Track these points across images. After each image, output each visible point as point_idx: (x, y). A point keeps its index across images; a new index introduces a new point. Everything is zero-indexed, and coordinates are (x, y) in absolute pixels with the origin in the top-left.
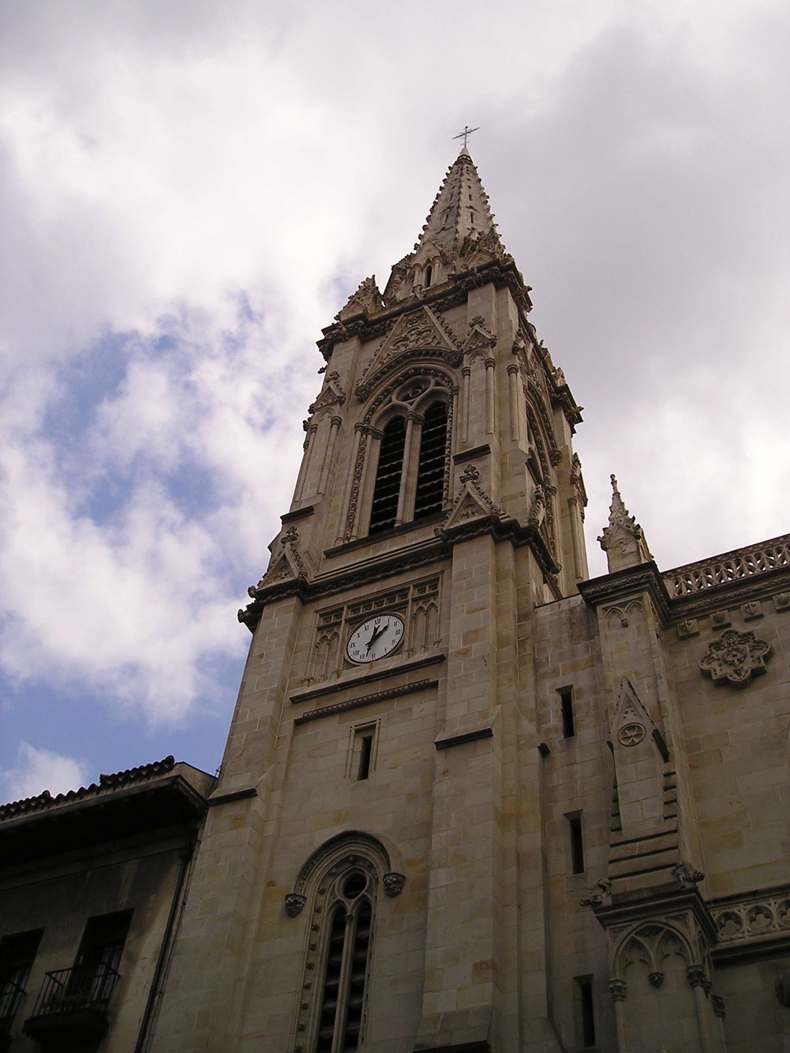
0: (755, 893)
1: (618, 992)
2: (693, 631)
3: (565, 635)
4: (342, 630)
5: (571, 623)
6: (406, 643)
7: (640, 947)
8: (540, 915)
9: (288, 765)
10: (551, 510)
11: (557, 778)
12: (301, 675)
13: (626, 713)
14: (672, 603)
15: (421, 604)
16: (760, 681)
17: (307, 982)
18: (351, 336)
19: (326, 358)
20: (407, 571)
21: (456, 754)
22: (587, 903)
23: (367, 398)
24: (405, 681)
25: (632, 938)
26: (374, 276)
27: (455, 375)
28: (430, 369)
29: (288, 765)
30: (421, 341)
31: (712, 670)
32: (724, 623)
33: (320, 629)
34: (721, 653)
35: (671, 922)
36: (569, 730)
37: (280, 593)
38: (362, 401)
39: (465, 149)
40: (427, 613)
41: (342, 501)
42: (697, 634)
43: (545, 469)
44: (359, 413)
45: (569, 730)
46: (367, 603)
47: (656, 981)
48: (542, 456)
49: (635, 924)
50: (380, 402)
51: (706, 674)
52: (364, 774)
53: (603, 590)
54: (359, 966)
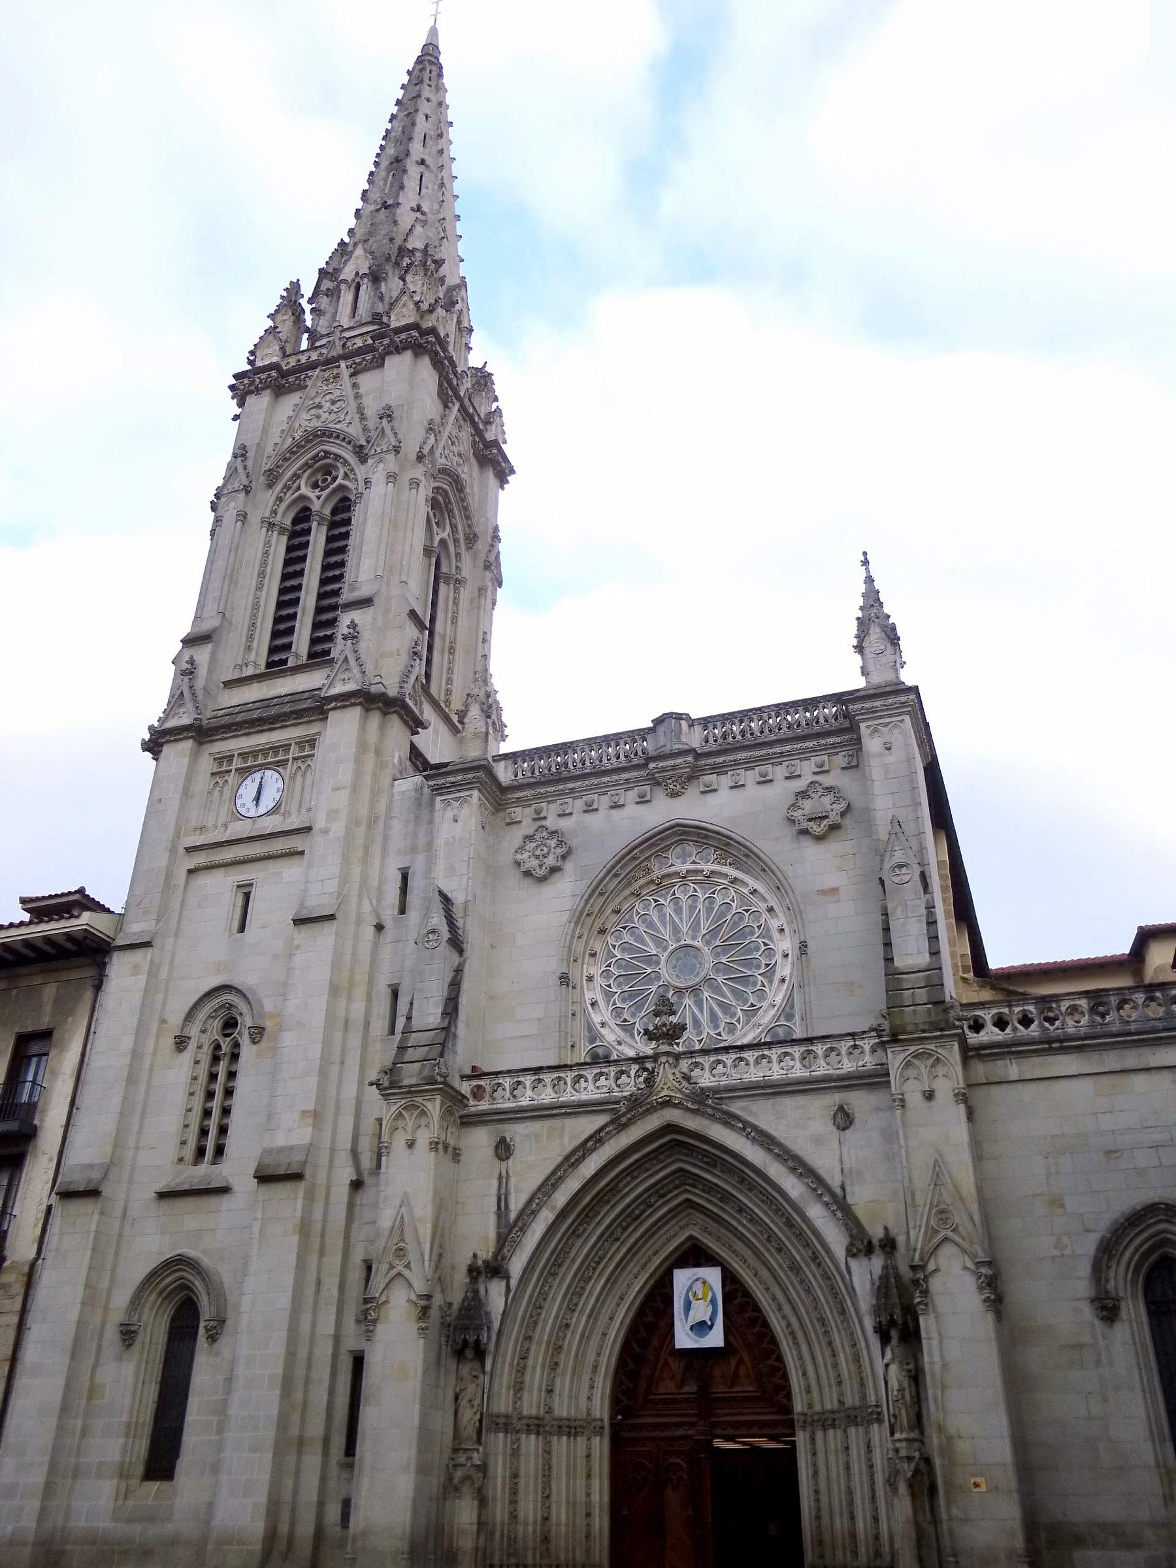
3: (412, 816)
4: (231, 778)
5: (418, 803)
6: (283, 804)
9: (181, 912)
10: (457, 607)
11: (386, 953)
12: (194, 822)
14: (504, 790)
15: (300, 764)
16: (557, 876)
17: (189, 1107)
18: (263, 389)
19: (241, 404)
20: (291, 725)
21: (306, 931)
23: (274, 483)
24: (279, 845)
26: (298, 280)
27: (361, 472)
28: (341, 457)
29: (181, 912)
30: (333, 416)
32: (542, 815)
33: (213, 774)
34: (534, 845)
36: (402, 911)
37: (178, 734)
38: (270, 486)
39: (434, 32)
40: (304, 776)
41: (241, 618)
42: (520, 822)
43: (458, 555)
44: (265, 501)
45: (402, 911)
46: (254, 754)
47: (411, 1144)
48: (456, 541)
49: (404, 1101)
50: (289, 489)
51: (518, 864)
52: (242, 929)
54: (229, 1093)
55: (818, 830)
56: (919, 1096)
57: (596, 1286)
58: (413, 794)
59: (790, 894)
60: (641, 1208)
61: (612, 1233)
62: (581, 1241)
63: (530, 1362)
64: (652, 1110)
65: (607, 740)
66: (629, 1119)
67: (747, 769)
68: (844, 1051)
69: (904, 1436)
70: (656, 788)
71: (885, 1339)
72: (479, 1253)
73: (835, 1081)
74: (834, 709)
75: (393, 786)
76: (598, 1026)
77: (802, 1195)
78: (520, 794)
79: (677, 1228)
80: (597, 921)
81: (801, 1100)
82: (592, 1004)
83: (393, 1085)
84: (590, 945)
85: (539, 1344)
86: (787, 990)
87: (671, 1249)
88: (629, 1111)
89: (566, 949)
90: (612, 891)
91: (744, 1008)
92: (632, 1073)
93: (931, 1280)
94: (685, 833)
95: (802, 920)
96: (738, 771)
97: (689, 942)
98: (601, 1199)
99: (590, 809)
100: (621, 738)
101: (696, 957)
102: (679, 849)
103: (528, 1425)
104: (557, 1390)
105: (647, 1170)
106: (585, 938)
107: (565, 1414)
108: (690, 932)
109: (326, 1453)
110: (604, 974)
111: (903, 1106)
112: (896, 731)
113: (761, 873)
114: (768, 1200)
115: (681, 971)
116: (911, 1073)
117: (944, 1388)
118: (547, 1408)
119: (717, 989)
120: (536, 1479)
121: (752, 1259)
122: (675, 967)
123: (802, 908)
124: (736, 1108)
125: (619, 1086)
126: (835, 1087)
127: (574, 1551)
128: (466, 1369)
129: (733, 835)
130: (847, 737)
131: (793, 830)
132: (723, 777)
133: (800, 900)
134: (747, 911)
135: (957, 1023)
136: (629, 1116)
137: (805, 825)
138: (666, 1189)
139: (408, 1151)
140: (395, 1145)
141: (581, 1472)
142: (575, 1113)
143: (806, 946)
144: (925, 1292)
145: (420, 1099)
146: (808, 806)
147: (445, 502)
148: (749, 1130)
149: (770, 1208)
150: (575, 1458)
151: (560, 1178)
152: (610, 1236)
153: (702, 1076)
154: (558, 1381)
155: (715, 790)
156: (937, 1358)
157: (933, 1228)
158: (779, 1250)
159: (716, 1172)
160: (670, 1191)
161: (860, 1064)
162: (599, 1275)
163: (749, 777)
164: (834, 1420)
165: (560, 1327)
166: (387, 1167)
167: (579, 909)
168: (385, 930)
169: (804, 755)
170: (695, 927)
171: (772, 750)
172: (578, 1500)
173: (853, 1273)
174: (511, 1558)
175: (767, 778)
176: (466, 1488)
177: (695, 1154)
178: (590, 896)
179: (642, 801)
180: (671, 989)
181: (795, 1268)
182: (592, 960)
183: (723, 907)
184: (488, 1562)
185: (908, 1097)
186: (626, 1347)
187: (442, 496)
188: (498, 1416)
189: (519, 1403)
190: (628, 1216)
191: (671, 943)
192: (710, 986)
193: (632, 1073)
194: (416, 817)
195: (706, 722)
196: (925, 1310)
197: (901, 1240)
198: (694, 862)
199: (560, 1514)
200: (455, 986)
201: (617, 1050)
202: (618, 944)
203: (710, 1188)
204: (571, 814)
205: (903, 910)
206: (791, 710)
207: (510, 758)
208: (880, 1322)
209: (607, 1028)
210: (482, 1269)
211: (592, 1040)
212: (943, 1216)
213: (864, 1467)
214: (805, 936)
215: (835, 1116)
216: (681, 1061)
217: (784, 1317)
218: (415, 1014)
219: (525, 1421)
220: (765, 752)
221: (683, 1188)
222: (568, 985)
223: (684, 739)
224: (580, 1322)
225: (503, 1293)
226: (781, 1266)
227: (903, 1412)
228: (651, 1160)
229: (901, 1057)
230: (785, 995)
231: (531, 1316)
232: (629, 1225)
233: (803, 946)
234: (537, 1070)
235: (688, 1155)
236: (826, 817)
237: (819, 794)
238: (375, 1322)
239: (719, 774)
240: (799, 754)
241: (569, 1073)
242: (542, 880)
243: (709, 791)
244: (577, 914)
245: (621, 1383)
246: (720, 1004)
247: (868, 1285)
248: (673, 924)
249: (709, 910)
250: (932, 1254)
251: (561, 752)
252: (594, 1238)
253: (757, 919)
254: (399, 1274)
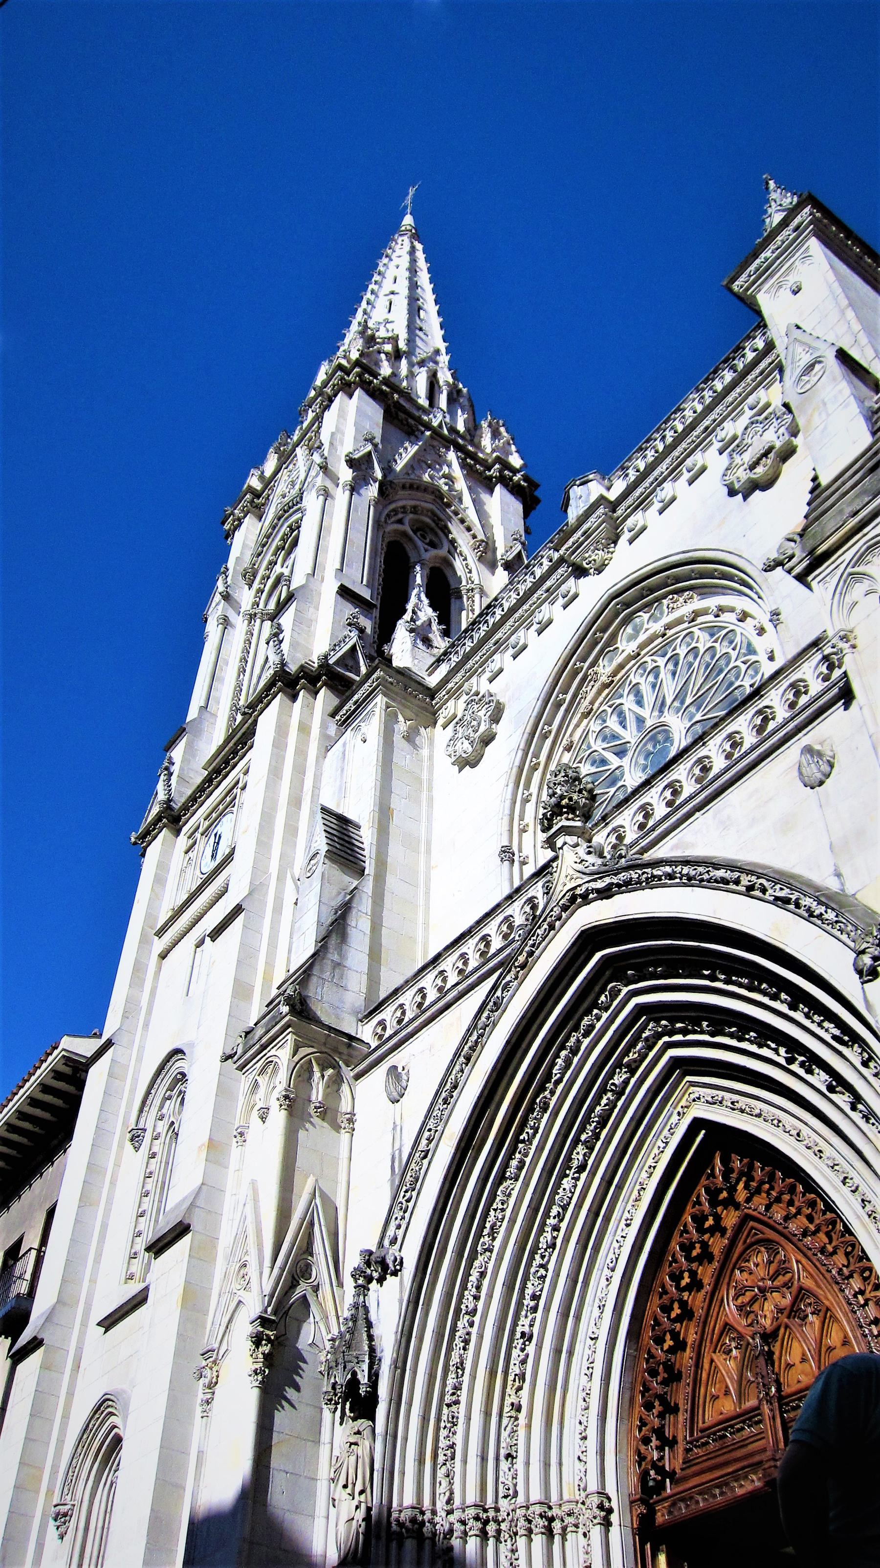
61: (569, 1158)
134: (715, 641)
147: (434, 521)
163: (677, 487)
187: (427, 516)
190: (587, 1120)
207: (443, 660)
221: (660, 1043)
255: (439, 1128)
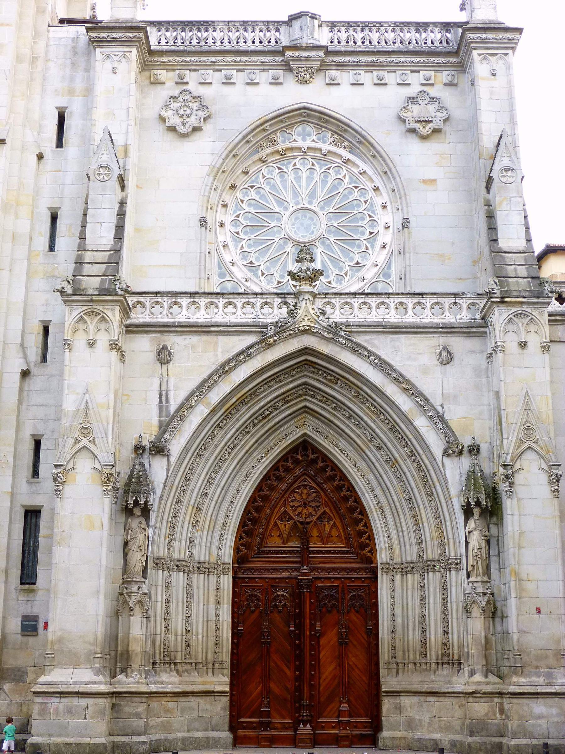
0: (157, 293)
1: (67, 346)
2: (162, 81)
3: (68, 62)
7: (86, 322)
8: (24, 278)
13: (103, 154)
14: (151, 52)
16: (198, 134)
22: (56, 291)
25: (81, 316)
31: (167, 119)
32: (185, 80)
34: (175, 105)
35: (105, 311)
36: (60, 143)
42: (164, 83)
45: (60, 143)
47: (91, 344)
49: (85, 308)
51: (163, 120)
53: (104, 38)
55: (424, 131)
56: (515, 345)
57: (230, 466)
58: (70, 42)
59: (398, 179)
60: (270, 410)
61: (246, 427)
62: (222, 432)
63: (180, 519)
64: (294, 335)
65: (245, 24)
66: (275, 341)
67: (366, 71)
68: (447, 306)
69: (479, 579)
70: (288, 74)
71: (468, 512)
72: (142, 434)
73: (441, 327)
74: (439, 36)
75: (48, 31)
76: (229, 265)
77: (410, 409)
78: (165, 59)
79: (294, 428)
80: (228, 179)
81: (414, 339)
82: (224, 246)
83: (77, 292)
84: (223, 197)
85: (187, 508)
86: (387, 254)
87: (289, 442)
88: (275, 334)
89: (206, 198)
90: (243, 155)
91: (352, 264)
92: (276, 305)
93: (516, 475)
94: (308, 115)
95: (406, 200)
96: (360, 72)
97: (307, 206)
98: (242, 401)
99: (228, 82)
100: (257, 25)
101: (312, 219)
102: (300, 129)
103: (177, 566)
104: (197, 541)
105: (281, 382)
106: (219, 191)
107: (202, 559)
108: (307, 198)
109: (6, 582)
110: (233, 222)
111: (503, 351)
112: (501, 62)
113: (371, 159)
114: (379, 411)
115: (298, 229)
116: (511, 327)
117: (520, 548)
118: (190, 553)
119: (329, 247)
120: (183, 603)
121: (353, 454)
122: (293, 224)
123: (406, 191)
124: (361, 339)
125: (263, 314)
126: (441, 332)
127: (207, 652)
128: (135, 523)
129: (352, 124)
130: (451, 60)
131: (403, 128)
132: (345, 74)
133: (405, 184)
134: (356, 187)
135: (550, 295)
136: (275, 338)
137: (413, 125)
138: (290, 398)
139: (89, 350)
140: (76, 343)
141: (213, 599)
142: (228, 332)
143: (408, 222)
144: (512, 484)
145: (101, 308)
146: (416, 111)
148: (373, 358)
149: (379, 416)
150: (208, 589)
151: (215, 381)
152: (244, 430)
153: (332, 314)
154: (198, 534)
155: (339, 84)
156: (517, 528)
157: (521, 440)
158: (379, 449)
159: (336, 388)
160: (294, 399)
161: (458, 317)
162: (232, 459)
164: (413, 568)
165: (202, 495)
166: (70, 361)
167: (218, 165)
168: (43, 161)
169: (416, 68)
170: (312, 195)
171: (390, 59)
172: (209, 619)
173: (447, 468)
174: (166, 658)
175: (383, 82)
176: (137, 610)
177: (320, 373)
178: (227, 156)
179: (276, 82)
180: (291, 242)
181: (392, 462)
182: (224, 209)
183: (336, 181)
184: (151, 661)
185: (506, 344)
186: (247, 511)
188: (158, 559)
189: (172, 549)
190: (260, 415)
191: (291, 205)
192: (323, 243)
193: (276, 305)
194: (73, 64)
195: (333, 25)
196: (511, 495)
197: (484, 448)
198: (313, 141)
199: (198, 628)
200: (121, 215)
201: (245, 286)
202: (246, 199)
203: (327, 398)
204: (210, 83)
205: (507, 204)
206: (406, 29)
207: (155, 25)
208: (468, 503)
209: (235, 266)
210: (147, 447)
211: (222, 275)
212: (528, 432)
213: (438, 600)
214: (408, 213)
215: (440, 353)
216: (316, 299)
217: (376, 496)
218: (88, 235)
219: (176, 563)
220: (384, 59)
222: (206, 228)
223: (316, 35)
224: (215, 492)
225: (166, 467)
226: (378, 460)
227: (480, 563)
228: (285, 374)
229: (505, 314)
230: (386, 258)
231: (182, 486)
232: (259, 422)
233: (406, 222)
234: (193, 294)
235: (313, 373)
236: (431, 121)
237: (426, 102)
238: (63, 483)
239: (342, 71)
240: (410, 66)
241: (221, 299)
242: (184, 136)
243: (333, 83)
244: (216, 170)
245: (241, 538)
246: (332, 259)
247: (458, 477)
248: (293, 190)
249: (324, 182)
250: (518, 457)
251: (202, 28)
252: (233, 431)
253: (363, 195)
254: (85, 447)
255: (202, 397)
